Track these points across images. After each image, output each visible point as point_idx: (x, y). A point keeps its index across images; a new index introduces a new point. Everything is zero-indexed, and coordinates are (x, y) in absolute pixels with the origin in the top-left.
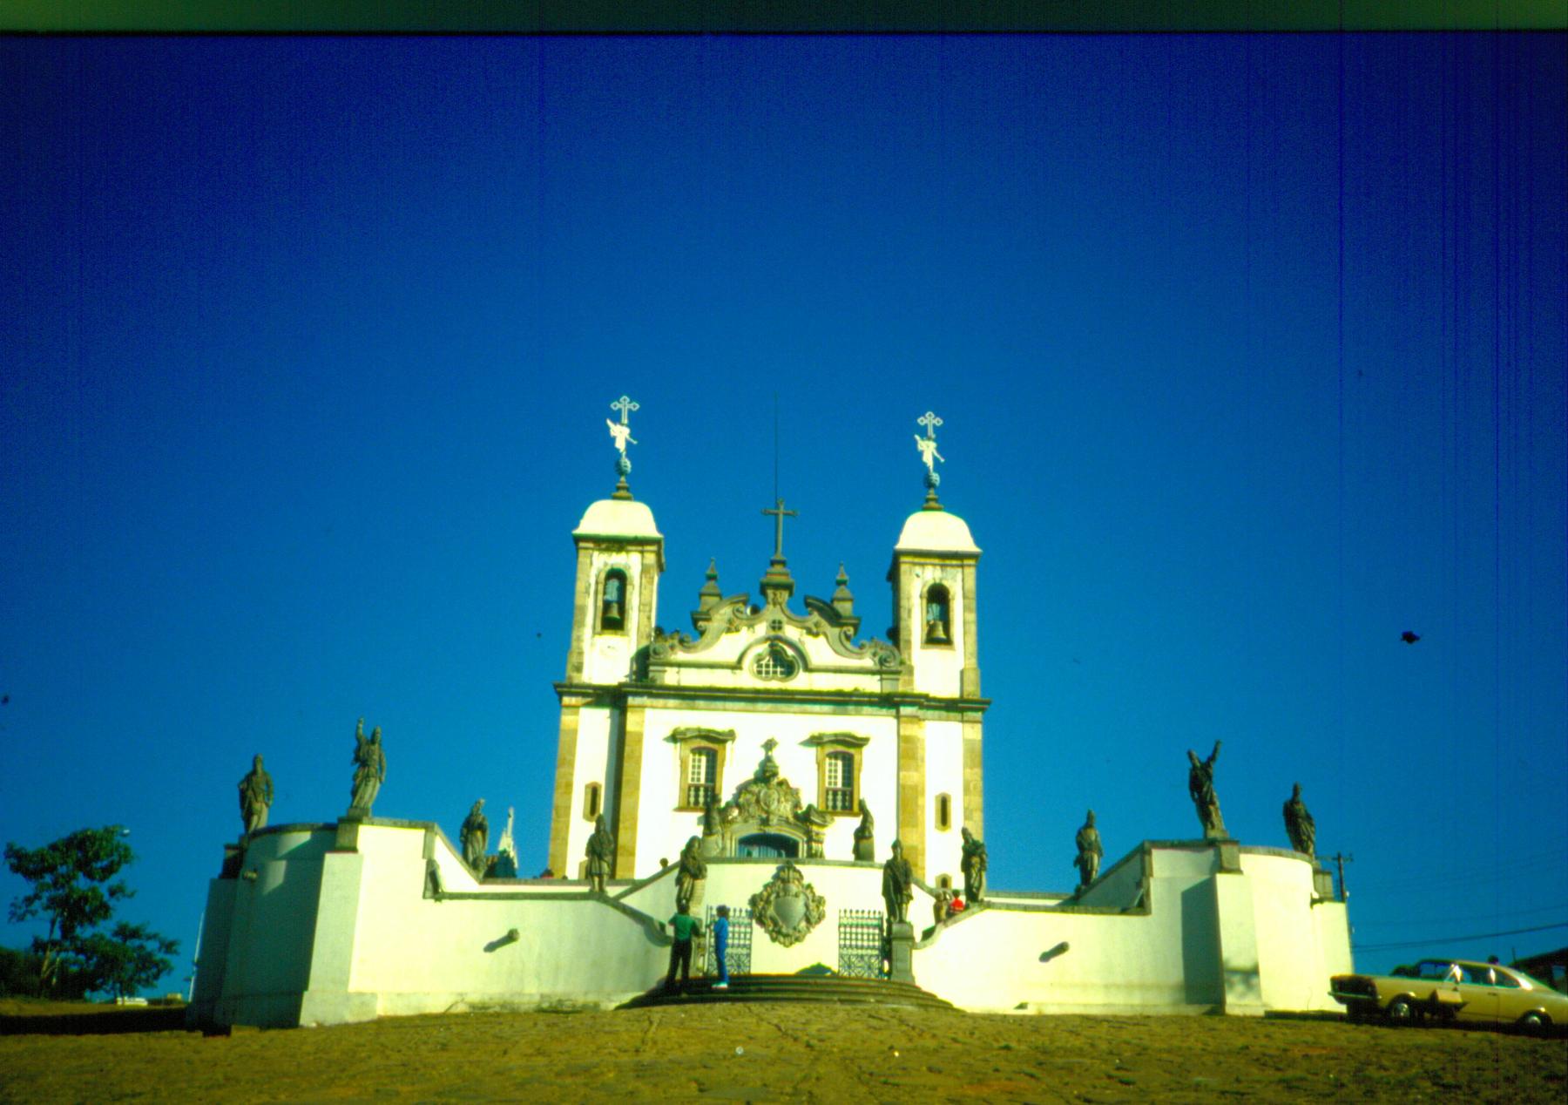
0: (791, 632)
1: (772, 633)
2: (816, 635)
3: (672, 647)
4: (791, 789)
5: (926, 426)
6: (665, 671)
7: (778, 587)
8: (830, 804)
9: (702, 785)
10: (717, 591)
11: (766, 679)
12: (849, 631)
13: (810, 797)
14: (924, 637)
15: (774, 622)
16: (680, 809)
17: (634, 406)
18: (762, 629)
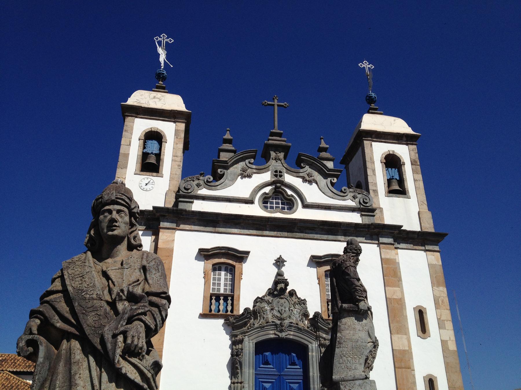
0: (288, 178)
1: (275, 179)
2: (310, 182)
3: (198, 185)
4: (299, 298)
5: (364, 67)
6: (192, 202)
7: (277, 148)
9: (222, 295)
10: (233, 148)
11: (271, 212)
12: (334, 180)
14: (387, 188)
15: (276, 171)
16: (203, 316)
18: (267, 177)
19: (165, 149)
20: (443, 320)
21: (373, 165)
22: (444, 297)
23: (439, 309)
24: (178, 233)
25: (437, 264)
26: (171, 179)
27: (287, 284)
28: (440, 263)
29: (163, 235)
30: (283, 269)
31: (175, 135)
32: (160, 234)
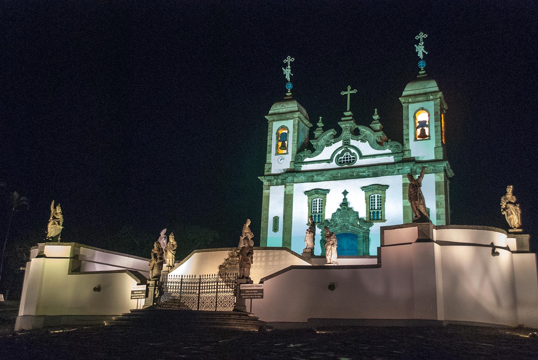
0: (353, 142)
6: (302, 167)
8: (372, 217)
13: (363, 214)
17: (293, 60)
18: (340, 144)
19: (288, 138)
20: (439, 215)
21: (407, 122)
22: (442, 201)
23: (438, 208)
24: (295, 184)
25: (441, 181)
26: (292, 155)
27: (347, 206)
28: (443, 180)
29: (288, 188)
30: (347, 196)
31: (293, 128)
32: (287, 187)
